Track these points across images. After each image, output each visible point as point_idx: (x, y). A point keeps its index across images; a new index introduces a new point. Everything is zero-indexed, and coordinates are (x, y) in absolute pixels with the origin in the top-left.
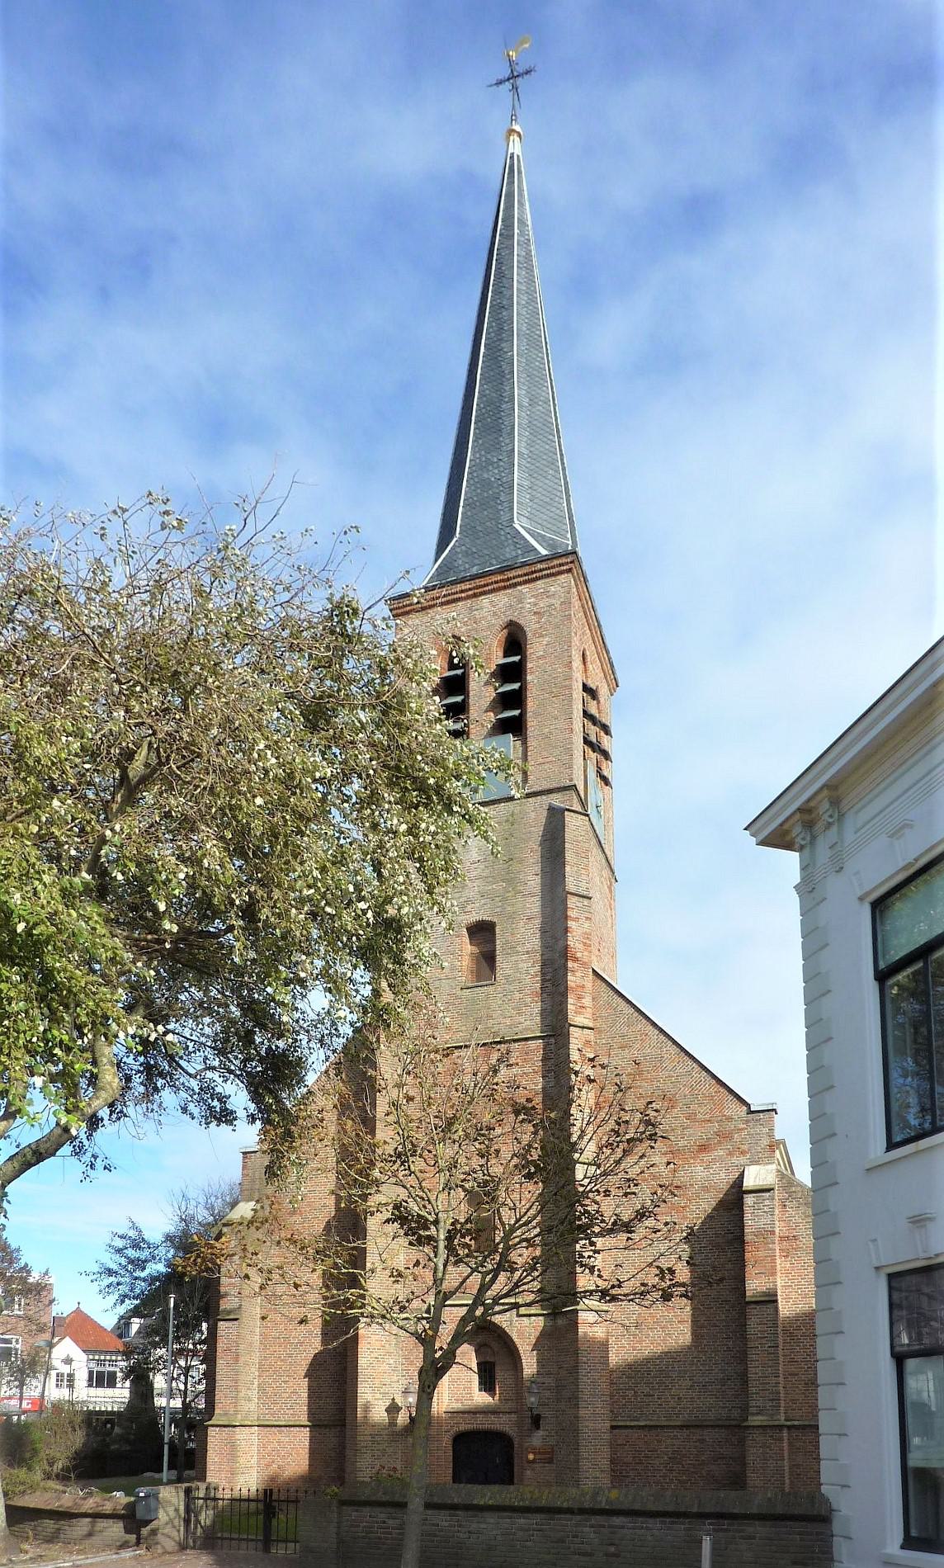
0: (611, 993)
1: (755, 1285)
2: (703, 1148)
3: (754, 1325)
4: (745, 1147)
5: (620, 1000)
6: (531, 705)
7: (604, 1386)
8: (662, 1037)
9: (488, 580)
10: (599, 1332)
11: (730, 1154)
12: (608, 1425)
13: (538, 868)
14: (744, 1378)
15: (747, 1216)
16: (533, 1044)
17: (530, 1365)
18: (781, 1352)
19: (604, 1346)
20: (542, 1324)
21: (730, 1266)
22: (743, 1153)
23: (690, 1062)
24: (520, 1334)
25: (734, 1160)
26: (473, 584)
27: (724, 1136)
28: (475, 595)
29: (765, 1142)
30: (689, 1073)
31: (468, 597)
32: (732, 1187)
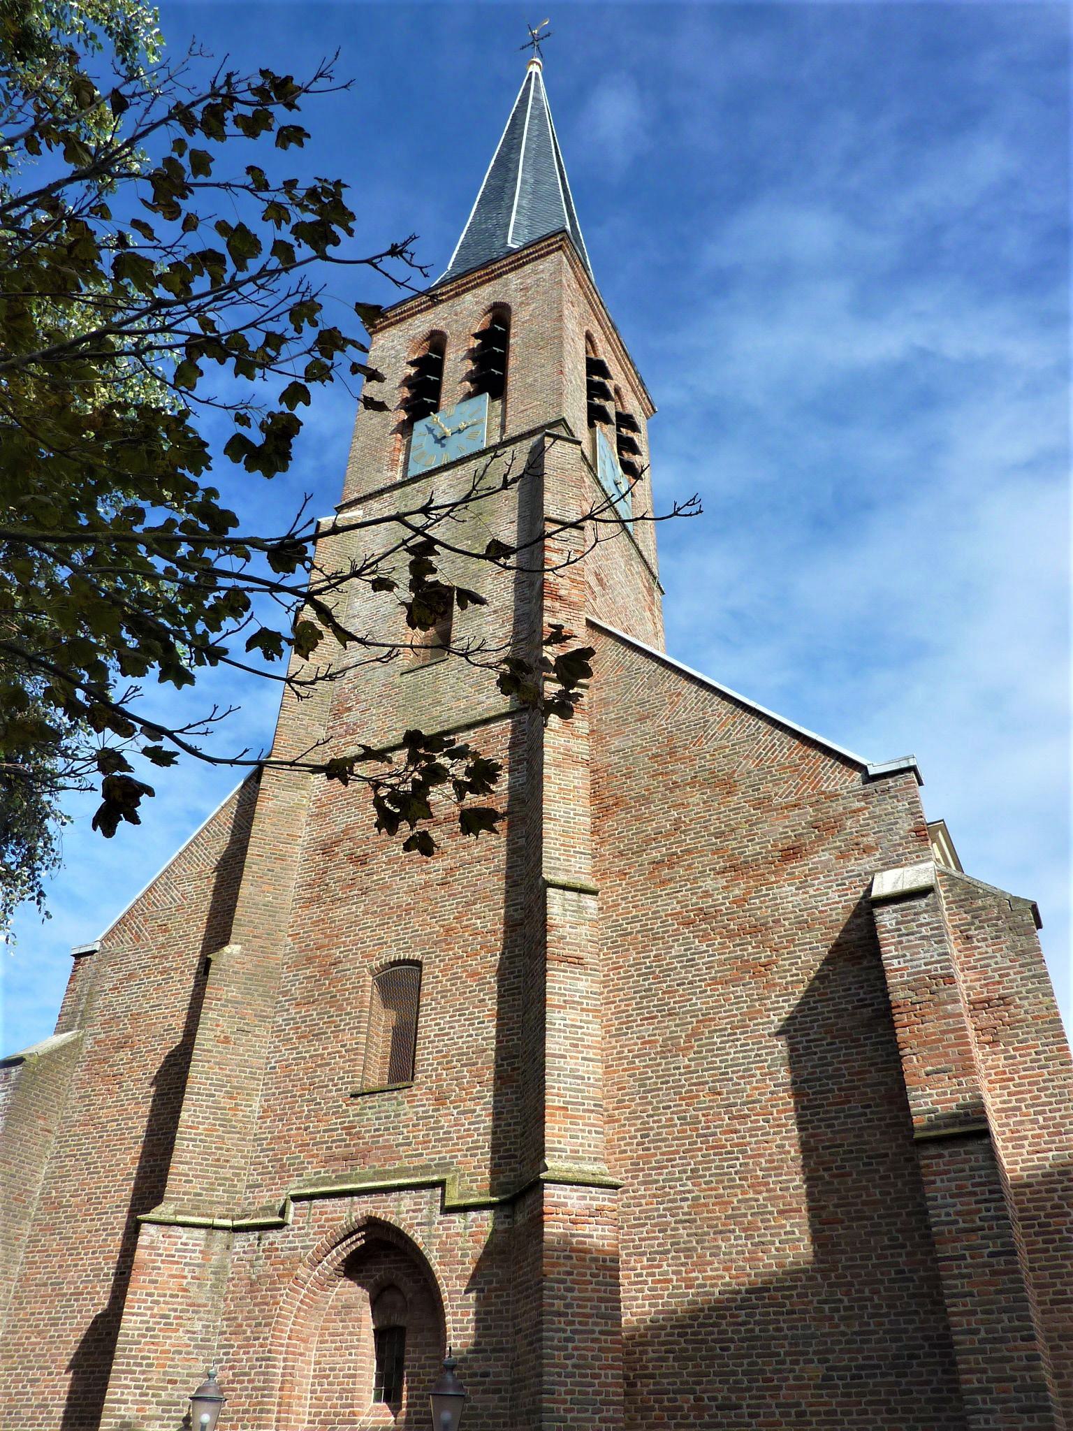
0: (622, 649)
1: (929, 1099)
2: (792, 853)
3: (943, 1179)
4: (870, 840)
5: (635, 656)
6: (512, 363)
7: (610, 1380)
8: (704, 694)
9: (471, 277)
10: (598, 1235)
11: (843, 856)
13: (514, 516)
14: (944, 1345)
15: (889, 951)
16: (495, 727)
17: (460, 1326)
18: (1028, 1278)
19: (606, 1268)
20: (488, 1227)
21: (873, 1076)
22: (867, 850)
23: (753, 721)
25: (852, 865)
26: (455, 285)
27: (826, 827)
28: (457, 295)
29: (906, 825)
30: (753, 737)
31: (450, 298)
32: (856, 914)
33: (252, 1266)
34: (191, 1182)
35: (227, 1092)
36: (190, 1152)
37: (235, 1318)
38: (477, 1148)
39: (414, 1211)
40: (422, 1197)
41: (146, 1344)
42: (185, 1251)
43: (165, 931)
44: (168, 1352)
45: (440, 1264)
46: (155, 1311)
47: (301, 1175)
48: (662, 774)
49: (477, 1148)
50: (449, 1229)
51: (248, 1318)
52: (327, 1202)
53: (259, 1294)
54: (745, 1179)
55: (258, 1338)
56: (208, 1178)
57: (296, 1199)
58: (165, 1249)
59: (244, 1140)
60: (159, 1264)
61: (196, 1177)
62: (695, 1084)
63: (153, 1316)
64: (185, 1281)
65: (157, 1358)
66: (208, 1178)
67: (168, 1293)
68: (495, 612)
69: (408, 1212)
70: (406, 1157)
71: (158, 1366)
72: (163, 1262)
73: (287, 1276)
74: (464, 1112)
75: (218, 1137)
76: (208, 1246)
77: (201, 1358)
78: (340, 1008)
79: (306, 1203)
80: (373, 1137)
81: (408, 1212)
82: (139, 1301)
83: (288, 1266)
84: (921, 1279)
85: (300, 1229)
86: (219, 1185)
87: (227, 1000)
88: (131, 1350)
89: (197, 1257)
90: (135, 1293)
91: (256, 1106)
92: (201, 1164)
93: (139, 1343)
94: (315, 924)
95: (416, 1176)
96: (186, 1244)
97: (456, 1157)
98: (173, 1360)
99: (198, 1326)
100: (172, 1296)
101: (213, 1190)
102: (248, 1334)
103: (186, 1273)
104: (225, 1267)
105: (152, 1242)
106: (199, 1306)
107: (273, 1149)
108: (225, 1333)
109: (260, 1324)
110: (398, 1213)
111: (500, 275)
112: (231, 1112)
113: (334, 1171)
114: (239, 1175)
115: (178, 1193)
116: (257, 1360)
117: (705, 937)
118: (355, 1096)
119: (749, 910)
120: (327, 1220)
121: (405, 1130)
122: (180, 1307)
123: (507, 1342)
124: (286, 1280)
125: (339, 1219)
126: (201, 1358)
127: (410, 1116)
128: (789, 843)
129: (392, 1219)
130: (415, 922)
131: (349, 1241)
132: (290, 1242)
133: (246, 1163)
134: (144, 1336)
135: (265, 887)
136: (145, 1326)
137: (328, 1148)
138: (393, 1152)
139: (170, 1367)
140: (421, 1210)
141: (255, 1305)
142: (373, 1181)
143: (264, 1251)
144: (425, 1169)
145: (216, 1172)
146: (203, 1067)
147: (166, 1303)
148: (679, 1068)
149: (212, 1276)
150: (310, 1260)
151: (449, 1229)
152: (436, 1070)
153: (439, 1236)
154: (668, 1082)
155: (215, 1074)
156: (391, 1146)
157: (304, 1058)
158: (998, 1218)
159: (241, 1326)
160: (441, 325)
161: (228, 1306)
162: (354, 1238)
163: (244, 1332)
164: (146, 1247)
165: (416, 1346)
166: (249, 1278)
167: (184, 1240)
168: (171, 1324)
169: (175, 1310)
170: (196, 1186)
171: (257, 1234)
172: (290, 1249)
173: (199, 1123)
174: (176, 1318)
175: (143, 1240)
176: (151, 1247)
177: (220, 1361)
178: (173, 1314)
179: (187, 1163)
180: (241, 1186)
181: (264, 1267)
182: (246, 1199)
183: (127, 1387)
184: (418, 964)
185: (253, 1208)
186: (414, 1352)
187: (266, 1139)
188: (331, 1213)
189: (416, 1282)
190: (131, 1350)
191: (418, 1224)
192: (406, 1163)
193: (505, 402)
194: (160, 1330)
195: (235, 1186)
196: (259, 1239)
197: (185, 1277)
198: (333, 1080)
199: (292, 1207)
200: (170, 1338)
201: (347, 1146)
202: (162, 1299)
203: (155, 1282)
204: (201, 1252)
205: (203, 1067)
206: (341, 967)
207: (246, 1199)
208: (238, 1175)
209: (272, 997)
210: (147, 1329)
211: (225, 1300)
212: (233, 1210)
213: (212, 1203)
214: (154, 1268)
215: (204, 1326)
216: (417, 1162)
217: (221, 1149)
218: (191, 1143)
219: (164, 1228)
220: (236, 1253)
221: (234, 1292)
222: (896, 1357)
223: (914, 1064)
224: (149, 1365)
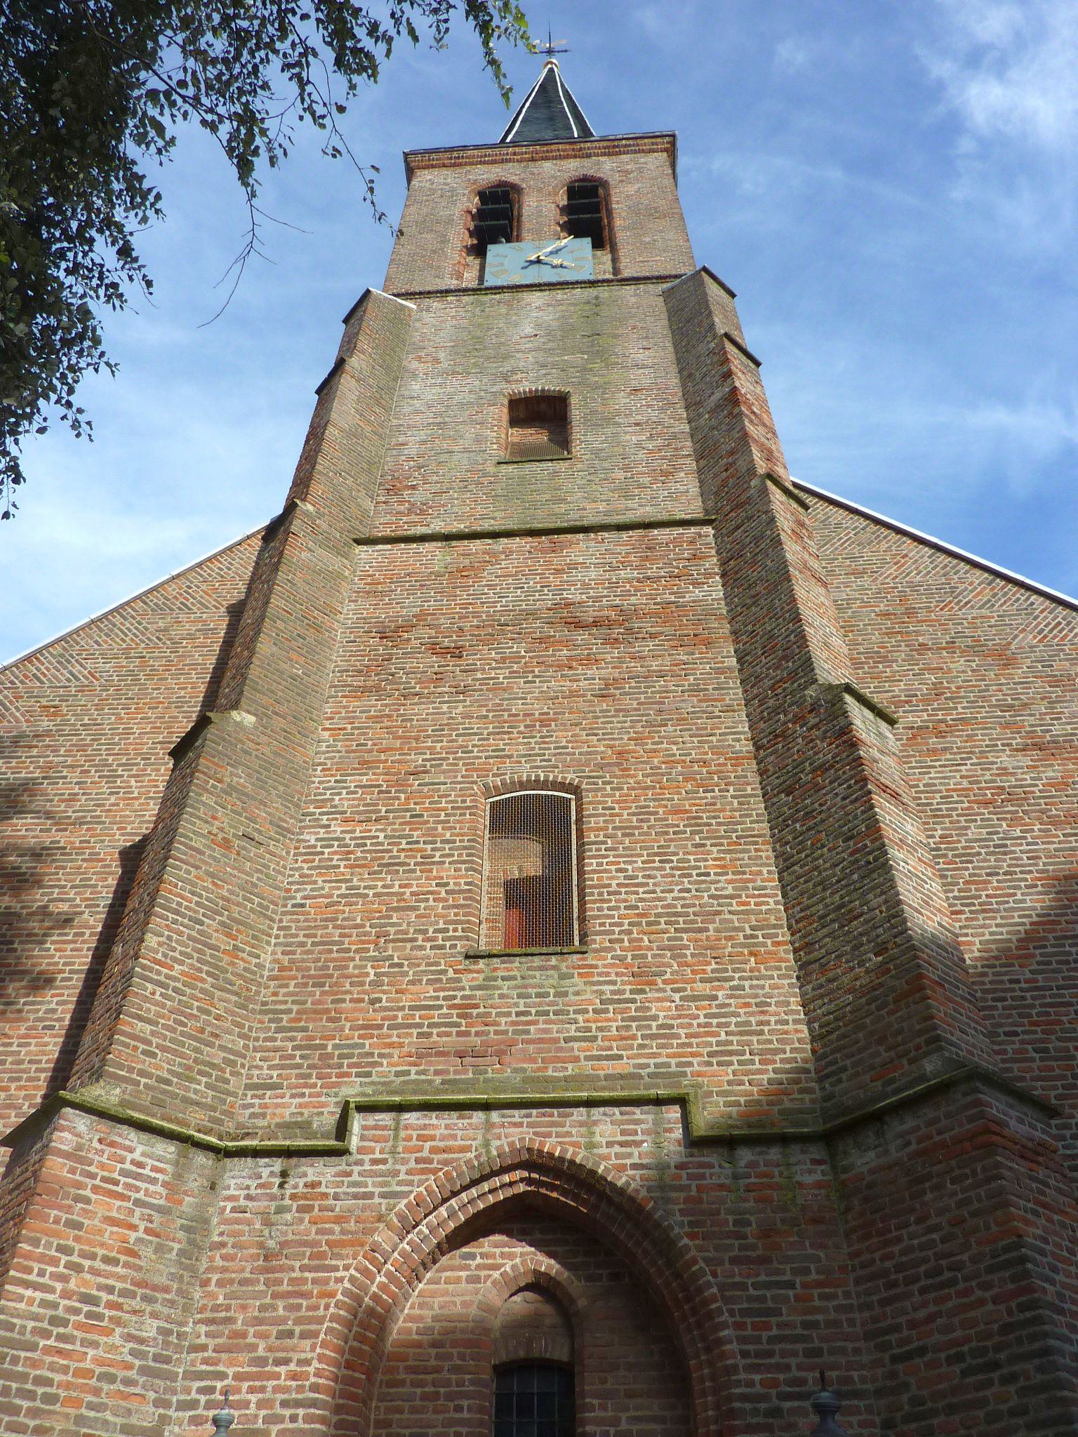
33: (267, 1223)
34: (154, 1055)
35: (222, 924)
36: (157, 1004)
37: (229, 1320)
38: (731, 1053)
39: (622, 1144)
40: (637, 1122)
41: (47, 1350)
42: (138, 1177)
43: (55, 714)
44: (88, 1373)
45: (692, 1236)
46: (72, 1285)
47: (369, 1075)
49: (731, 1053)
50: (703, 1177)
51: (258, 1321)
52: (433, 1118)
53: (285, 1277)
55: (286, 1362)
56: (182, 1056)
58: (102, 1166)
59: (244, 1007)
60: (87, 1193)
61: (164, 1049)
62: (1051, 1005)
63: (66, 1295)
64: (133, 1236)
65: (68, 1386)
66: (182, 1056)
67: (101, 1252)
68: (637, 424)
69: (610, 1144)
70: (587, 1058)
71: (68, 1401)
72: (95, 1189)
73: (352, 1244)
74: (694, 998)
75: (202, 991)
76: (178, 1176)
77: (152, 1395)
78: (431, 832)
79: (386, 1118)
80: (514, 1023)
81: (610, 1144)
82: (42, 1259)
83: (352, 1226)
85: (374, 1162)
86: (201, 1073)
87: (229, 785)
88: (15, 1360)
89: (157, 1193)
90: (36, 1242)
91: (266, 959)
92: (174, 1030)
93: (33, 1347)
94: (378, 719)
95: (613, 1090)
96: (140, 1165)
97: (690, 1064)
98: (97, 1392)
99: (150, 1329)
100: (107, 1260)
101: (191, 1080)
102: (261, 1352)
103: (135, 1220)
104: (206, 1221)
105: (79, 1147)
106: (155, 1288)
107: (305, 1029)
108: (204, 1348)
109: (290, 1334)
110: (591, 1146)
111: (589, 156)
112: (226, 958)
113: (437, 1073)
114: (232, 1064)
115: (131, 1070)
116: (284, 1404)
117: (1014, 821)
118: (472, 957)
120: (433, 1150)
121: (580, 1018)
122: (119, 1285)
123: (863, 1380)
124: (348, 1251)
125: (463, 1149)
126: (152, 1395)
127: (588, 996)
130: (562, 737)
131: (474, 1192)
132: (355, 1184)
133: (246, 1047)
134: (46, 1334)
135: (294, 655)
136: (50, 1312)
137: (420, 1035)
138: (561, 1049)
139: (91, 1406)
140: (638, 1144)
141: (275, 1296)
143: (293, 1197)
145: (196, 1050)
146: (189, 873)
147: (94, 1272)
148: (1018, 981)
149: (181, 1235)
150: (402, 1217)
151: (703, 1177)
152: (630, 932)
154: (1004, 999)
155: (205, 889)
156: (556, 1040)
159: (244, 1335)
160: (513, 179)
161: (213, 1296)
162: (486, 1186)
163: (254, 1347)
164: (66, 1155)
165: (604, 1395)
166: (261, 1245)
167: (137, 1156)
168: (100, 1317)
169: (110, 1290)
170: (162, 1065)
171: (278, 1164)
172: (356, 1196)
173: (174, 960)
174: (111, 1305)
175: (63, 1139)
176: (74, 1156)
177: (193, 1404)
178: (104, 1296)
179: (149, 1021)
181: (294, 1226)
182: (245, 1107)
184: (576, 790)
185: (261, 1123)
186: (603, 1408)
187: (289, 1011)
188: (443, 1138)
189: (590, 1278)
190: (15, 1360)
192: (587, 1067)
193: (614, 250)
194: (79, 1326)
195: (227, 1082)
196: (284, 1174)
197: (133, 1228)
198: (425, 932)
199: (357, 1123)
200: (95, 1345)
201: (459, 1034)
202: (87, 1263)
203: (78, 1226)
204: (165, 1184)
205: (189, 873)
207: (245, 1107)
208: (232, 1064)
209: (298, 806)
210: (54, 1321)
211: (205, 1283)
212: (219, 1122)
213: (186, 1100)
214: (78, 1199)
215: (161, 1331)
217: (208, 1013)
218: (159, 990)
219: (104, 1125)
221: (224, 1270)
224: (51, 1399)
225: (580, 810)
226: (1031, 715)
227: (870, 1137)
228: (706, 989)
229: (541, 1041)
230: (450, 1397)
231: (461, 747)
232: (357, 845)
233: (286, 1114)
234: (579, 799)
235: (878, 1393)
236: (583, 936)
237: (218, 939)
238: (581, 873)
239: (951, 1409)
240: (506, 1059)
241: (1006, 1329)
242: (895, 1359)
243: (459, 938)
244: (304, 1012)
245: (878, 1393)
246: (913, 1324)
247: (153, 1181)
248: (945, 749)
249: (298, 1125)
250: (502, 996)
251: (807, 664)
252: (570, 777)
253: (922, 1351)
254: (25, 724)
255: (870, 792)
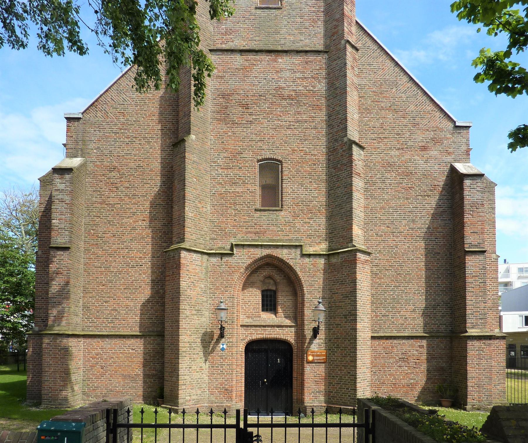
4: (451, 150)
12: (370, 335)
24: (303, 269)
27: (436, 141)
37: (215, 284)
38: (312, 236)
48: (377, 101)
49: (312, 236)
54: (396, 255)
57: (237, 245)
74: (305, 223)
83: (236, 268)
84: (444, 287)
89: (199, 263)
91: (209, 208)
99: (203, 286)
119: (406, 166)
125: (257, 254)
128: (423, 144)
129: (280, 256)
137: (246, 228)
140: (291, 254)
141: (224, 280)
142: (268, 242)
144: (290, 240)
153: (299, 263)
157: (230, 192)
158: (484, 274)
165: (282, 296)
170: (194, 237)
180: (208, 238)
183: (186, 305)
184: (280, 161)
189: (280, 276)
191: (291, 259)
203: (188, 270)
206: (242, 156)
207: (210, 243)
208: (206, 234)
213: (200, 244)
216: (287, 238)
220: (211, 262)
222: (434, 305)
223: (468, 231)
224: (191, 298)
225: (282, 169)
226: (404, 138)
227: (336, 257)
228: (307, 220)
229: (272, 231)
230: (254, 295)
231: (250, 145)
232: (226, 177)
233: (220, 245)
234: (282, 165)
235: (329, 298)
236: (282, 205)
237: (199, 205)
238: (282, 188)
239: (340, 302)
240: (265, 234)
241: (351, 292)
242: (333, 294)
243: (253, 205)
244: (220, 222)
245: (329, 298)
246: (336, 289)
247: (198, 261)
248: (378, 148)
249: (222, 248)
250: (264, 220)
251: (346, 128)
252: (280, 158)
253: (337, 293)
254: (116, 120)
255: (352, 177)
